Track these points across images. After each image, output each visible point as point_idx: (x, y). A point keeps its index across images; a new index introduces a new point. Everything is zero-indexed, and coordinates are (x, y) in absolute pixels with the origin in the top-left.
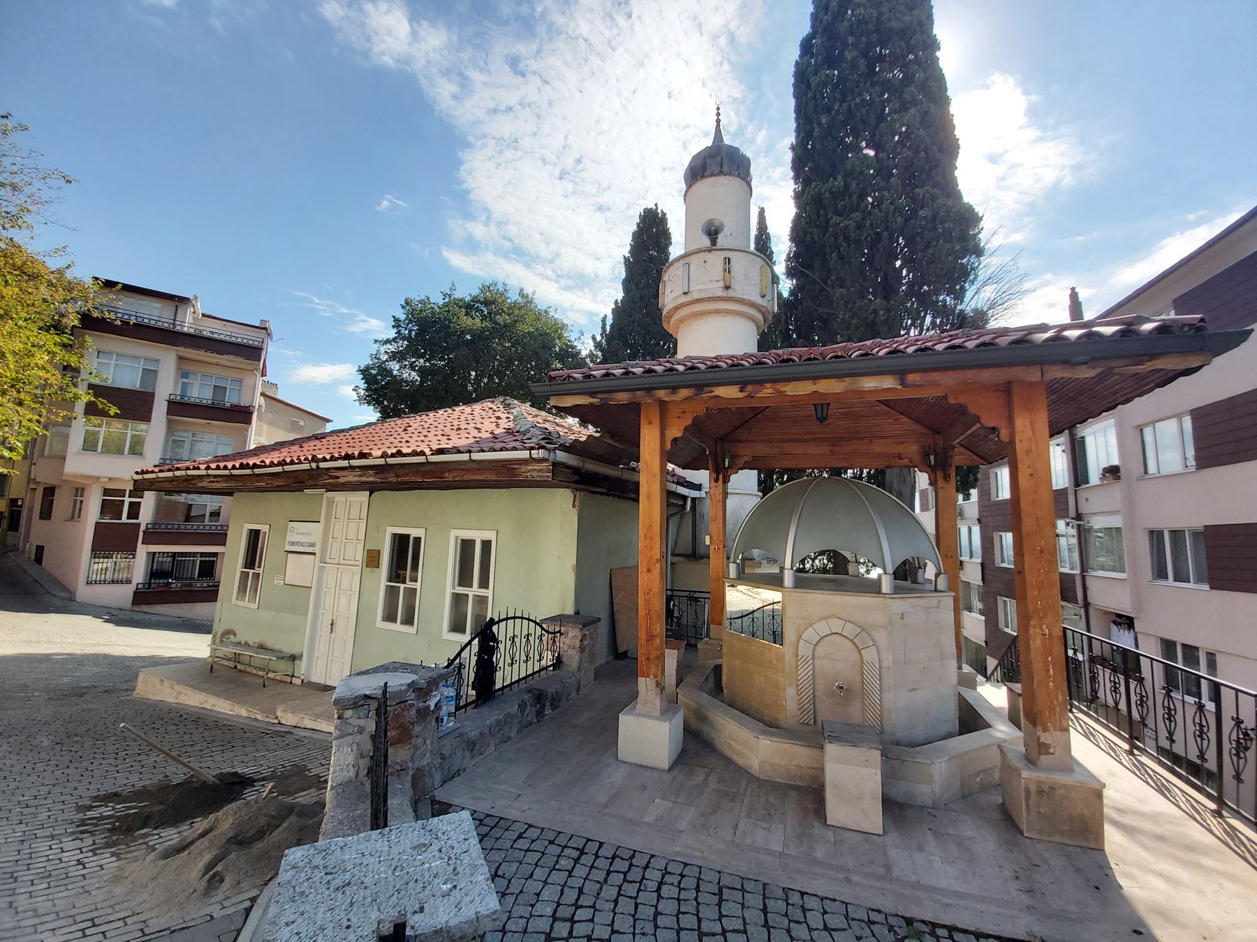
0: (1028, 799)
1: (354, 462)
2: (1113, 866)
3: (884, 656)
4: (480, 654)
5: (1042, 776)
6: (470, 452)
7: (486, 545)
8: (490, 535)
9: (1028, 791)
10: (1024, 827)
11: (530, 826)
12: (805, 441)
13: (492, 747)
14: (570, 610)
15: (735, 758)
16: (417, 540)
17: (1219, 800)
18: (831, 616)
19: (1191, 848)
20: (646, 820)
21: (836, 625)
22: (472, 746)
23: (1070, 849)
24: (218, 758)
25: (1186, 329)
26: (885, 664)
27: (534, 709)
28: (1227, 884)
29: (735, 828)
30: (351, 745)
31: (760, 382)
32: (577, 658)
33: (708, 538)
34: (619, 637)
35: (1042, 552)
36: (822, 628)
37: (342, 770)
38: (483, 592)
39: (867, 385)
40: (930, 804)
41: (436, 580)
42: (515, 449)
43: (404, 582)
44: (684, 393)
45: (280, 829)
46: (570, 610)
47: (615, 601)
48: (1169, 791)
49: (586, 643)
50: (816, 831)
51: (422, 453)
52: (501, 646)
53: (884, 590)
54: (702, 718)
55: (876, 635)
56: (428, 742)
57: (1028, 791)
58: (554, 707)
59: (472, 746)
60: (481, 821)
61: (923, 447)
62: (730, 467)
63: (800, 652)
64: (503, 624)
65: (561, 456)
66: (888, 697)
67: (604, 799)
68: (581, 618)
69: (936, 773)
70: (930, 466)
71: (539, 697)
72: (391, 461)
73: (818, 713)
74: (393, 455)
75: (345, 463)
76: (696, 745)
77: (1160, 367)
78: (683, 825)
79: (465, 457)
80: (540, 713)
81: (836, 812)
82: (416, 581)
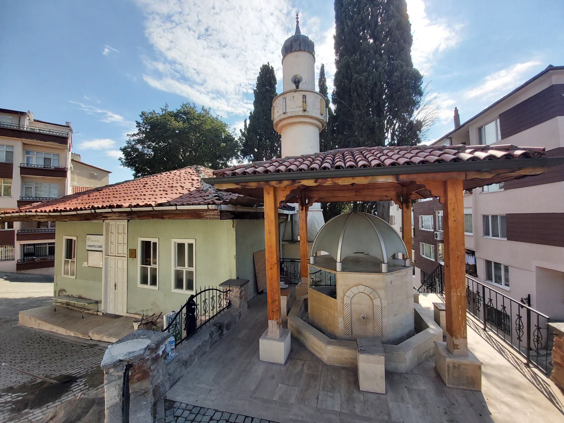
0: (448, 370)
1: (114, 210)
2: (486, 400)
3: (383, 302)
4: (187, 314)
5: (456, 360)
6: (176, 205)
7: (191, 246)
8: (192, 241)
9: (448, 366)
10: (447, 382)
11: (216, 411)
12: (343, 190)
13: (197, 359)
14: (234, 277)
15: (316, 353)
16: (155, 244)
17: (528, 359)
18: (359, 285)
19: (517, 386)
20: (275, 399)
21: (361, 288)
22: (186, 364)
23: (466, 392)
24: (59, 364)
25: (536, 154)
26: (383, 305)
27: (218, 334)
28: (536, 408)
29: (317, 398)
30: (115, 386)
31: (325, 178)
32: (238, 302)
33: (299, 237)
34: (259, 284)
35: (458, 257)
36: (355, 290)
37: (111, 399)
38: (190, 269)
39: (379, 180)
40: (404, 372)
41: (166, 264)
42: (199, 204)
43: (150, 265)
44: (285, 183)
45: (89, 414)
46: (234, 277)
47: (256, 268)
48: (504, 352)
49: (242, 294)
50: (355, 395)
51: (150, 206)
52: (199, 307)
53: (383, 271)
54: (299, 332)
55: (379, 292)
56: (160, 371)
57: (448, 366)
58: (228, 329)
59: (186, 364)
60: (191, 411)
61: (397, 193)
62: (308, 203)
63: (345, 302)
64: (199, 296)
65: (224, 207)
66: (385, 320)
67: (253, 388)
68: (239, 282)
69: (407, 356)
70: (400, 202)
71: (220, 327)
72: (134, 209)
73: (353, 329)
74: (135, 206)
75: (109, 210)
76: (297, 347)
77: (524, 174)
78: (292, 400)
79: (174, 208)
80: (221, 335)
81: (364, 385)
82: (156, 264)
